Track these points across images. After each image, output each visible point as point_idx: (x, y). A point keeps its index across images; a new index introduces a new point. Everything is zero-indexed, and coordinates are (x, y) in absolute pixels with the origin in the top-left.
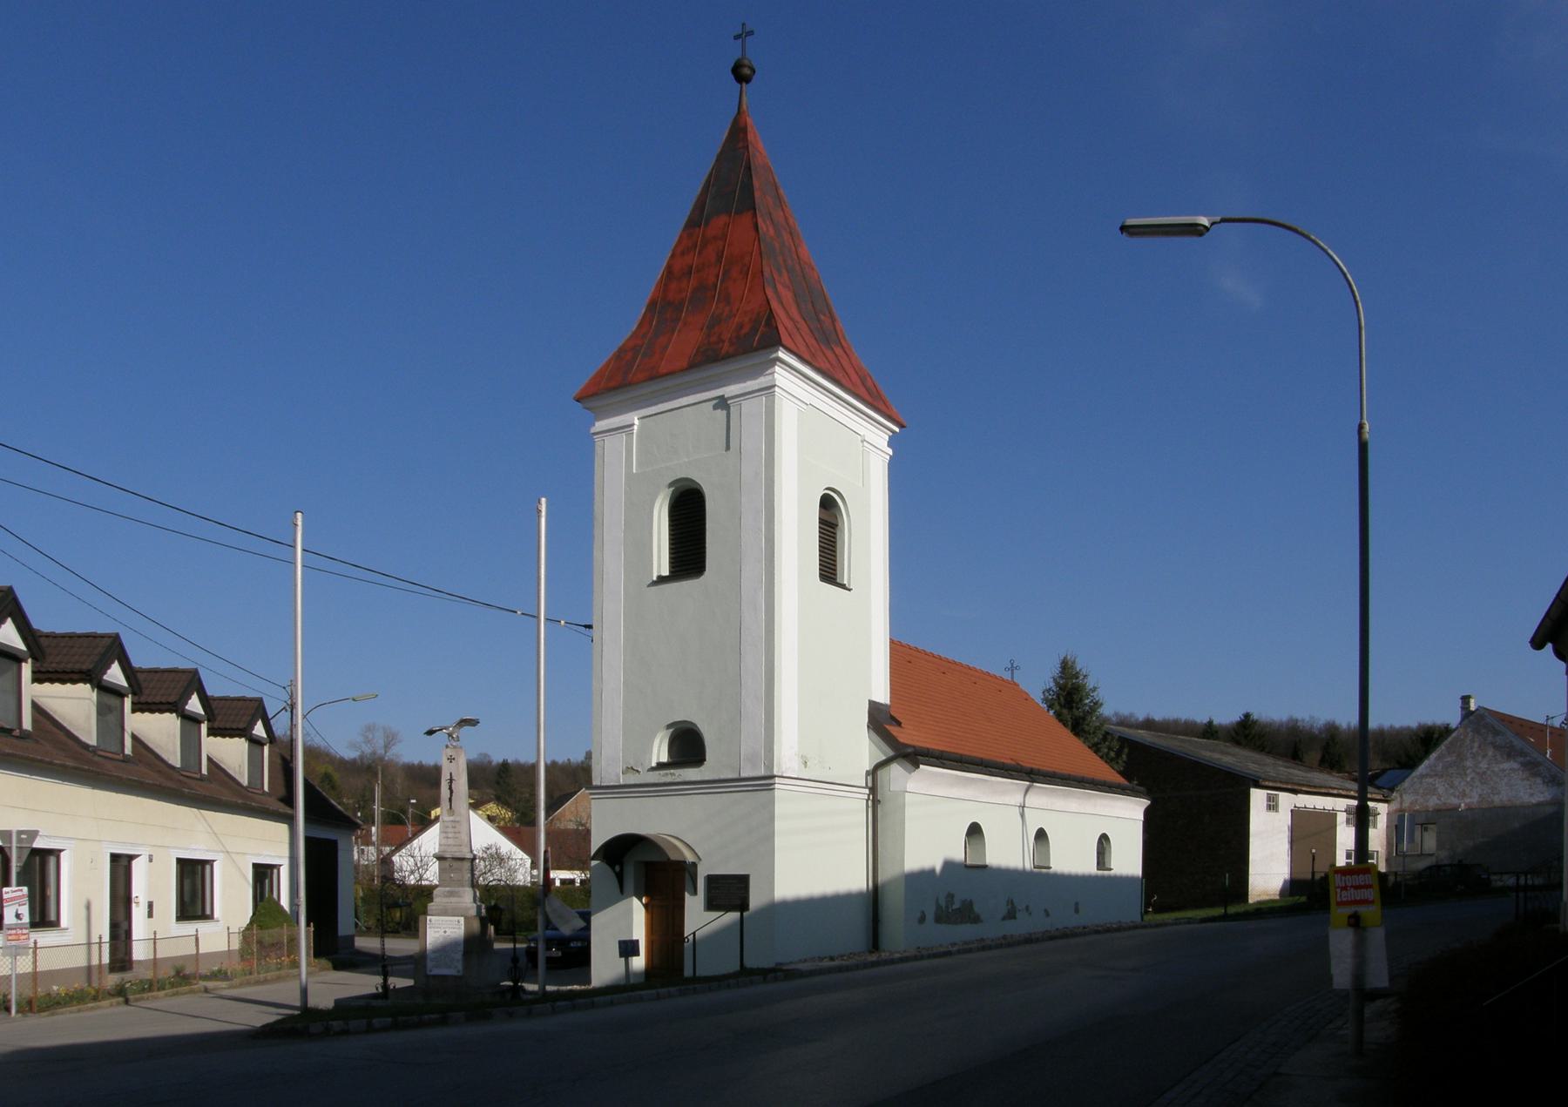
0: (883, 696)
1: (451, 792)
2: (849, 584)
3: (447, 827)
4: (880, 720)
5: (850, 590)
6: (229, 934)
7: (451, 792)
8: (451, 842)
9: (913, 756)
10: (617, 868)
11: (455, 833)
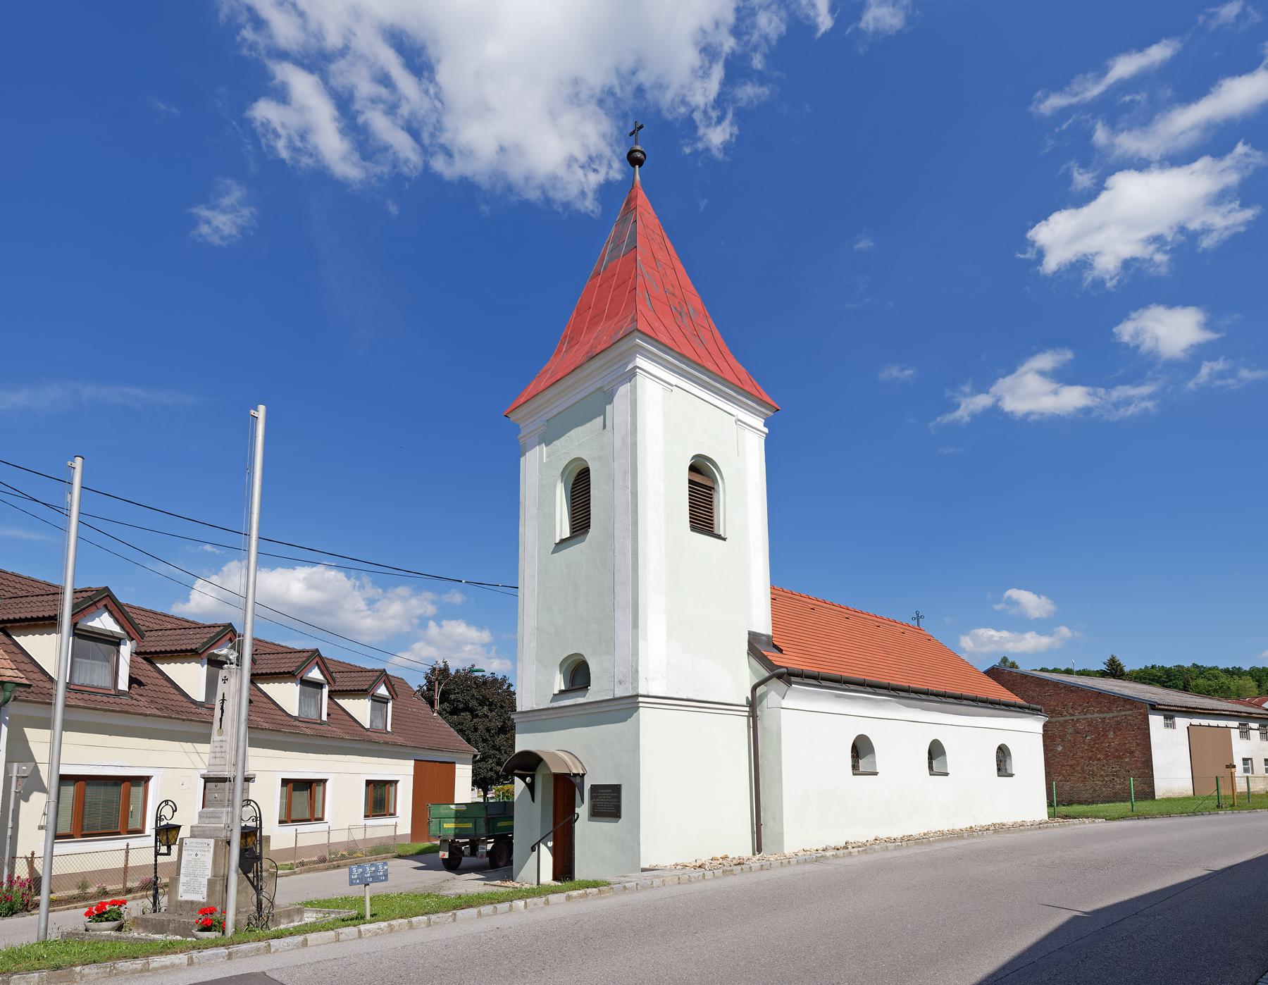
0: (764, 626)
1: (223, 712)
2: (725, 534)
3: (216, 747)
4: (756, 645)
5: (724, 539)
6: (296, 834)
7: (223, 712)
8: (218, 761)
9: (788, 677)
10: (528, 779)
11: (221, 752)
